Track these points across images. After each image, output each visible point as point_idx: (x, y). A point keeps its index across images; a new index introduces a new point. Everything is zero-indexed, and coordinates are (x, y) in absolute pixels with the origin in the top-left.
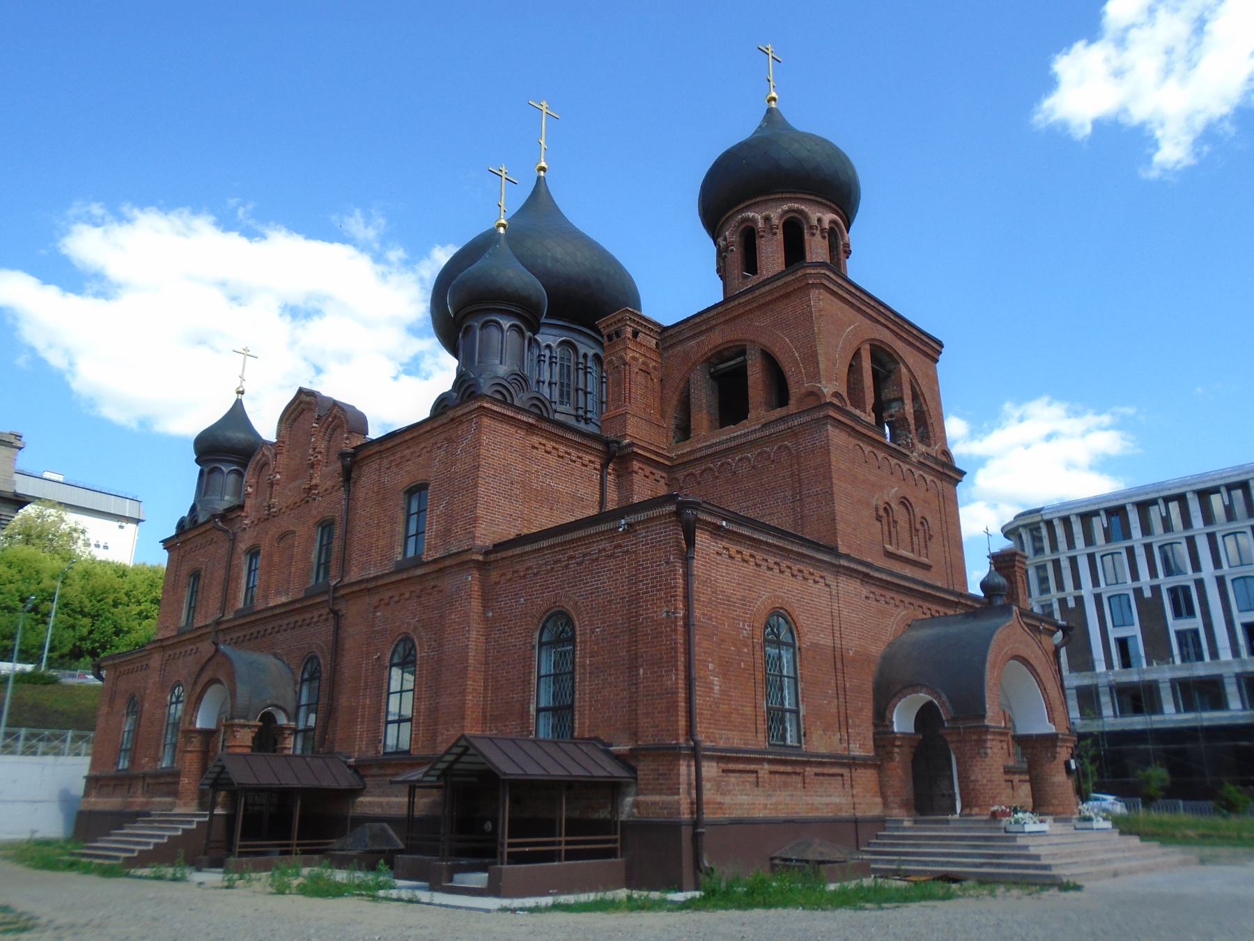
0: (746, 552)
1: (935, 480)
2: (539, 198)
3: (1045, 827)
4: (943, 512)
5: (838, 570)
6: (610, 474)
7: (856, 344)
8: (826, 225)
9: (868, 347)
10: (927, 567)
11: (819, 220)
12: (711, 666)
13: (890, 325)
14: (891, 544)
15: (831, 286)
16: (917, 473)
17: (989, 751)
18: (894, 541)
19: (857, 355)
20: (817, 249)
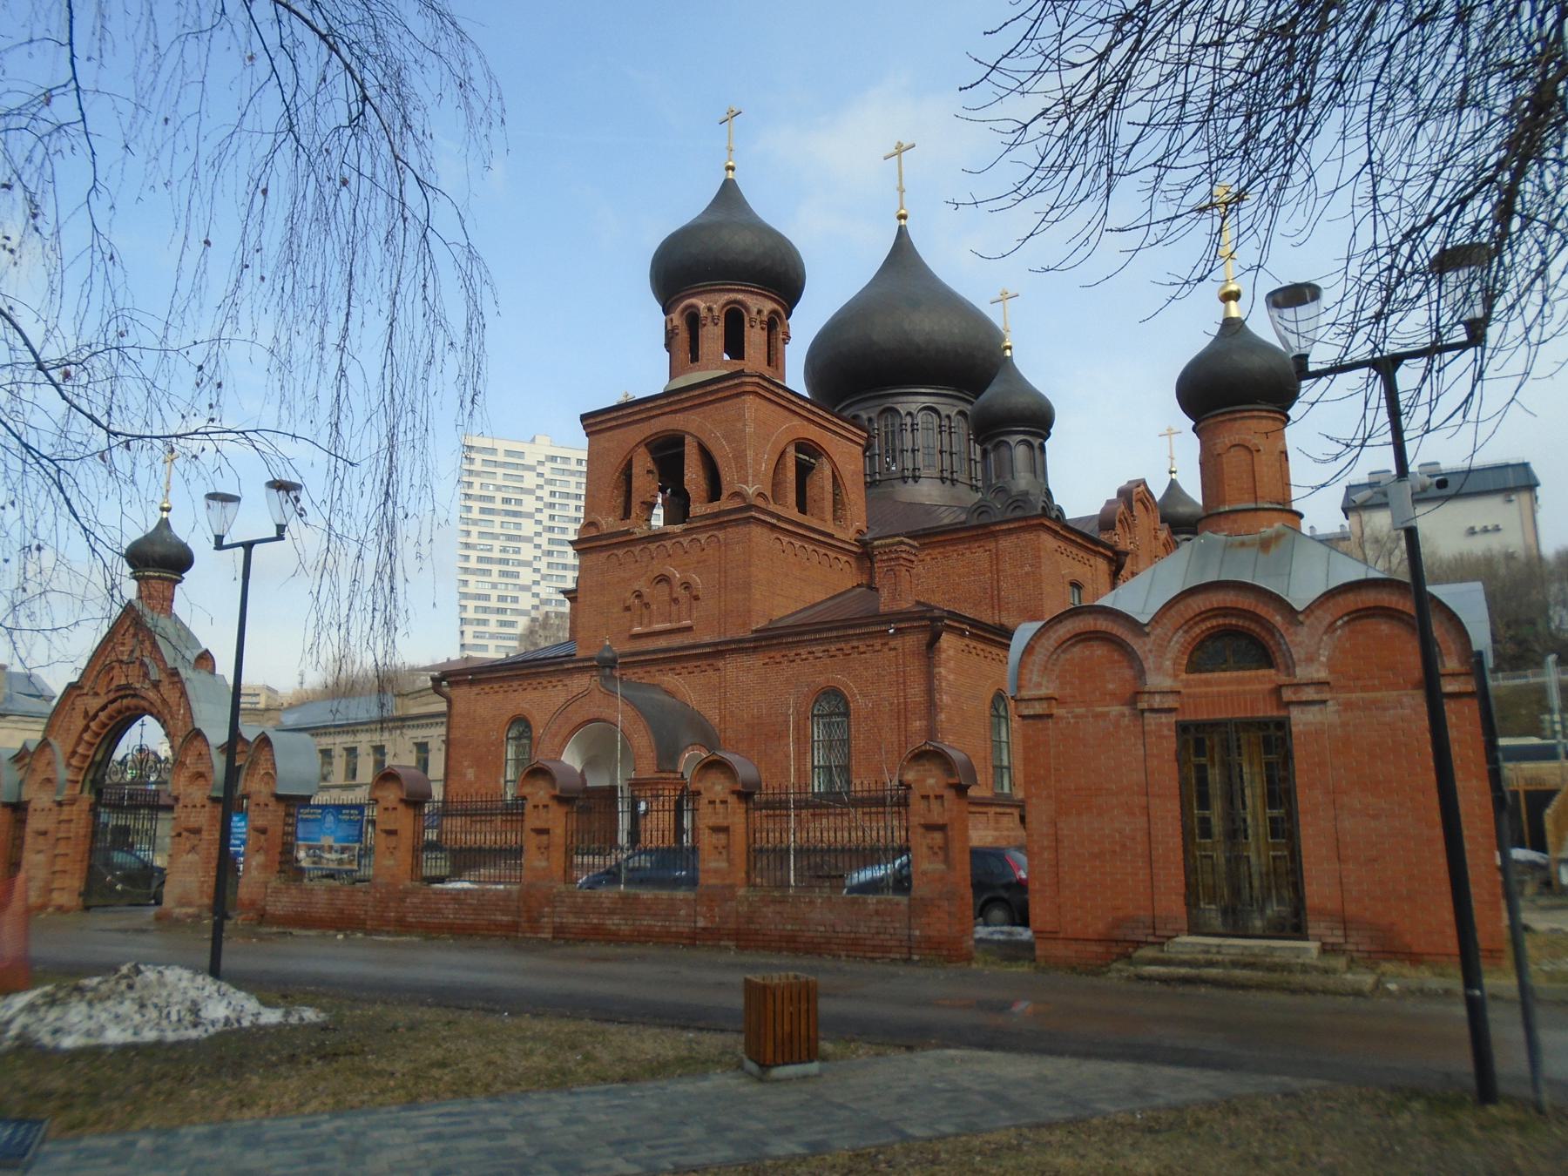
0: (496, 686)
2: (902, 253)
5: (570, 672)
9: (642, 449)
10: (689, 629)
12: (466, 764)
13: (667, 409)
14: (641, 624)
16: (685, 541)
18: (646, 621)
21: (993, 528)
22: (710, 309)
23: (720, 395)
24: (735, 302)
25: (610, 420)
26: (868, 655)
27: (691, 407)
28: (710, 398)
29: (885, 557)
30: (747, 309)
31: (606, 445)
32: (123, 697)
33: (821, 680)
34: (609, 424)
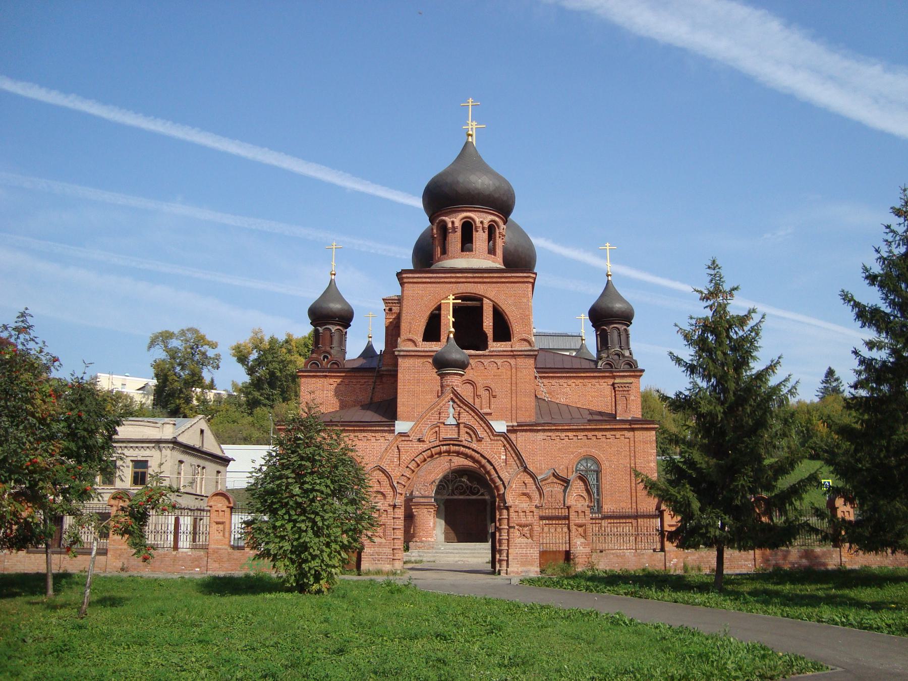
1: (509, 360)
3: (689, 551)
4: (514, 378)
6: (379, 385)
7: (432, 306)
8: (458, 224)
11: (453, 223)
15: (411, 280)
17: (415, 513)
19: (439, 308)
20: (455, 240)
21: (615, 374)
22: (482, 222)
23: (511, 280)
24: (494, 221)
25: (425, 278)
26: (611, 440)
27: (489, 282)
28: (503, 280)
29: (625, 389)
30: (499, 227)
31: (420, 292)
32: (443, 445)
33: (583, 451)
34: (424, 280)
